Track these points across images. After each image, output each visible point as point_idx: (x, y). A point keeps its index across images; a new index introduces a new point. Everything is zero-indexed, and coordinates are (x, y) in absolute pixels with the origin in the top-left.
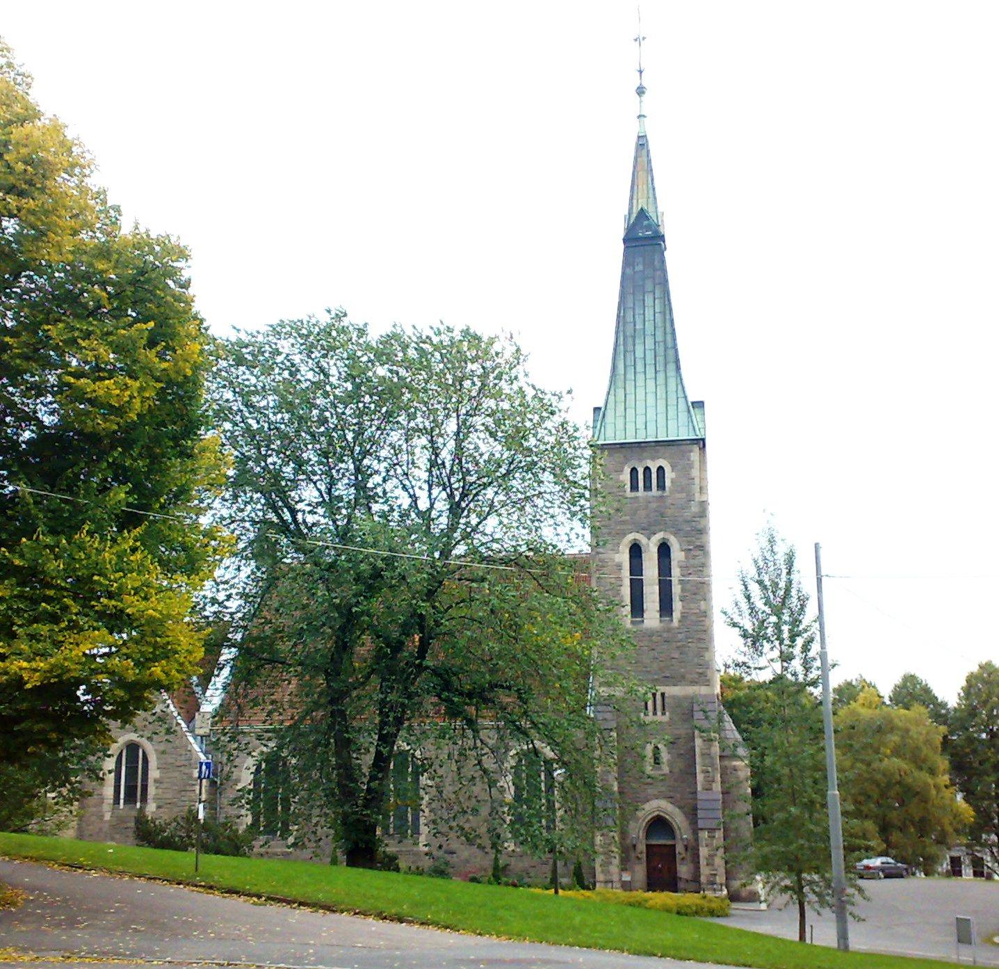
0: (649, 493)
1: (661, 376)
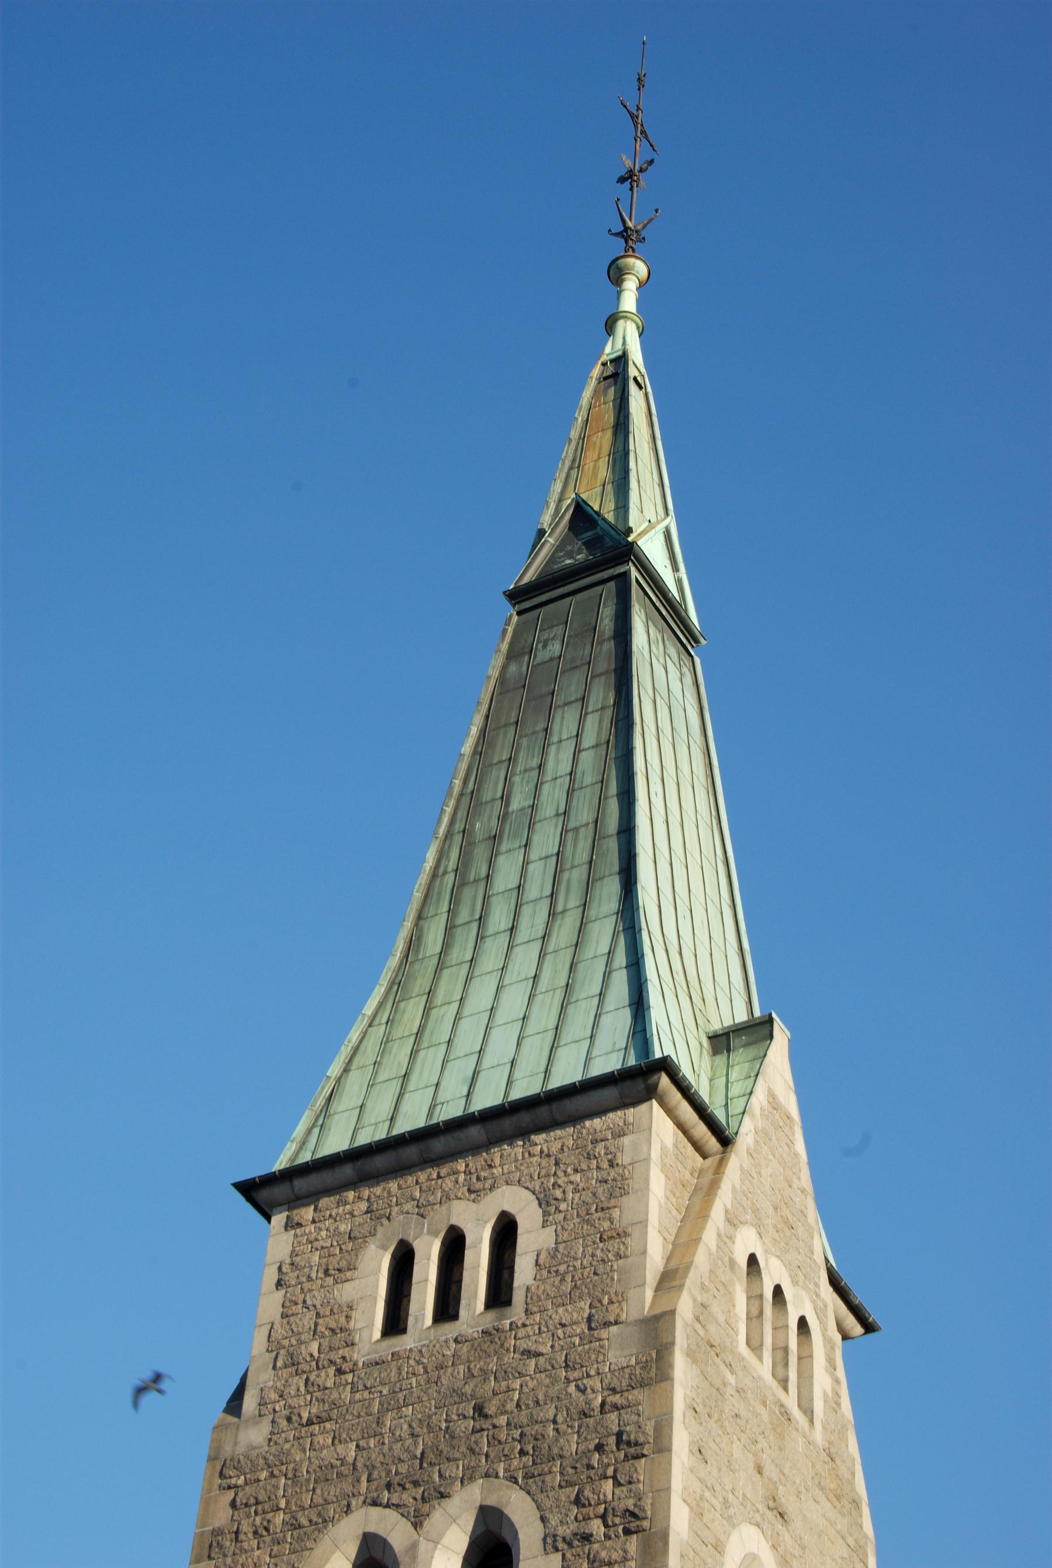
0: (450, 1330)
1: (564, 933)
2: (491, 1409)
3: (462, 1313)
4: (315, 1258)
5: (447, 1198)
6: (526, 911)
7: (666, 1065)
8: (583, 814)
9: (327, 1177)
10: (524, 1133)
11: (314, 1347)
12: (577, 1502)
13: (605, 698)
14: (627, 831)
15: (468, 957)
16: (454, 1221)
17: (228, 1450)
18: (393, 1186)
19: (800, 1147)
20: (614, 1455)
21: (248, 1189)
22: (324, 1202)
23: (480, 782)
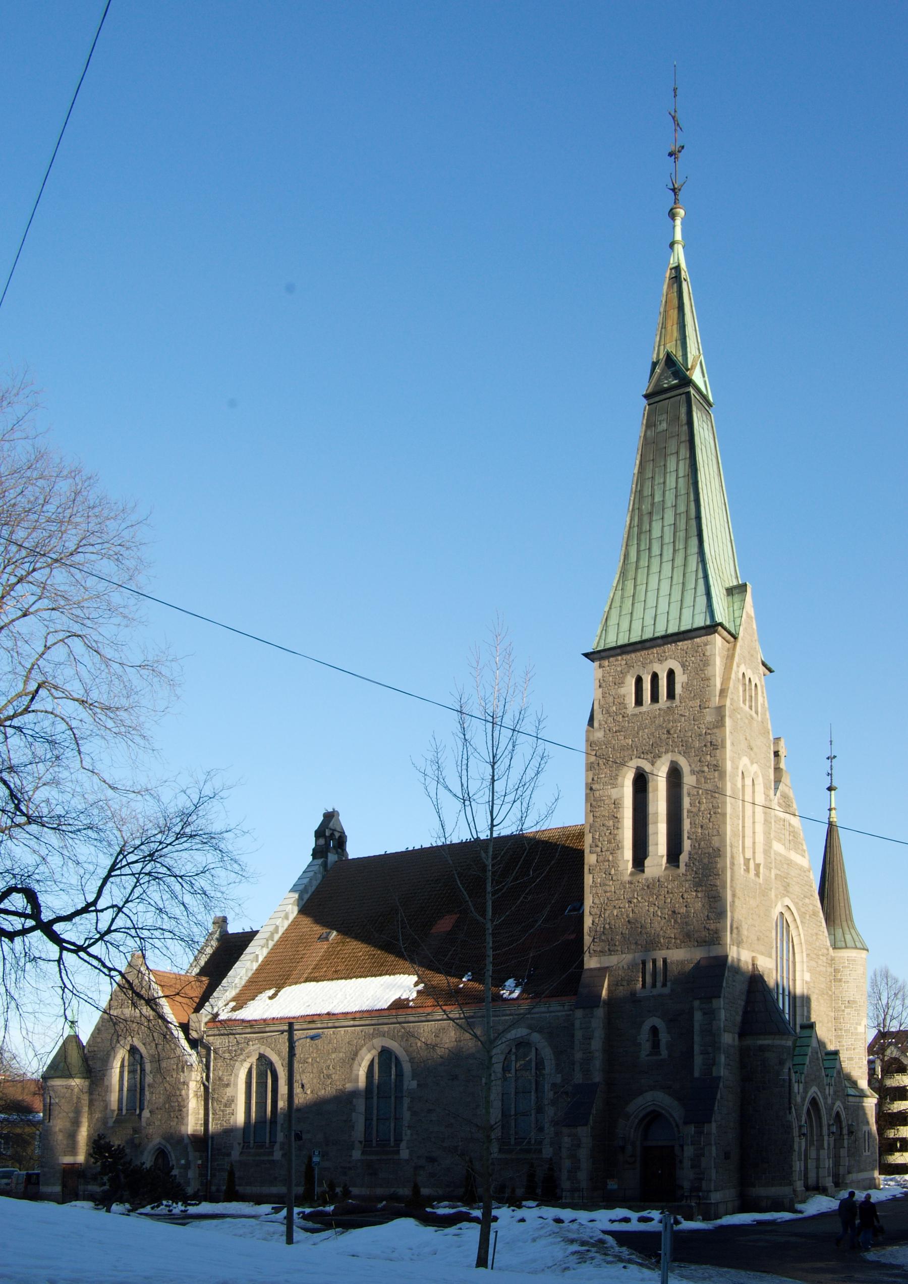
0: (656, 706)
2: (672, 732)
3: (660, 701)
4: (611, 679)
5: (651, 662)
6: (665, 547)
7: (721, 624)
8: (682, 508)
9: (612, 652)
10: (675, 642)
11: (614, 708)
12: (700, 761)
13: (686, 454)
14: (698, 518)
15: (647, 565)
16: (655, 670)
17: (591, 738)
18: (633, 655)
19: (755, 626)
20: (710, 748)
21: (586, 655)
22: (611, 659)
23: (642, 486)
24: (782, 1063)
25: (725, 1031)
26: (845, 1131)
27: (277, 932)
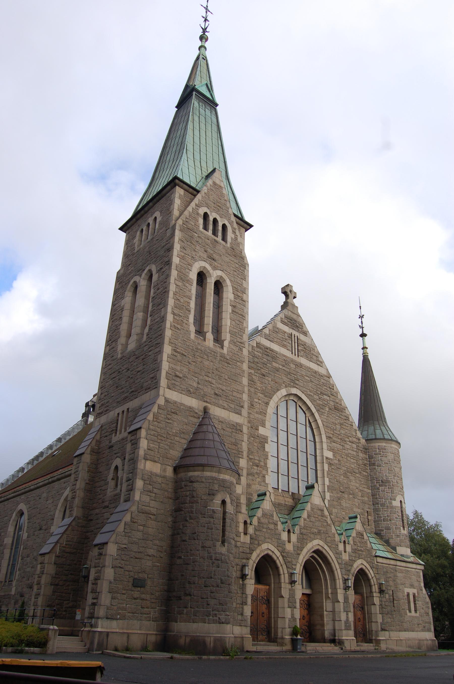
24: (212, 494)
25: (146, 459)
26: (375, 588)
27: (42, 456)
